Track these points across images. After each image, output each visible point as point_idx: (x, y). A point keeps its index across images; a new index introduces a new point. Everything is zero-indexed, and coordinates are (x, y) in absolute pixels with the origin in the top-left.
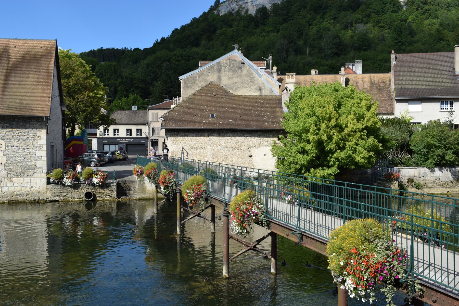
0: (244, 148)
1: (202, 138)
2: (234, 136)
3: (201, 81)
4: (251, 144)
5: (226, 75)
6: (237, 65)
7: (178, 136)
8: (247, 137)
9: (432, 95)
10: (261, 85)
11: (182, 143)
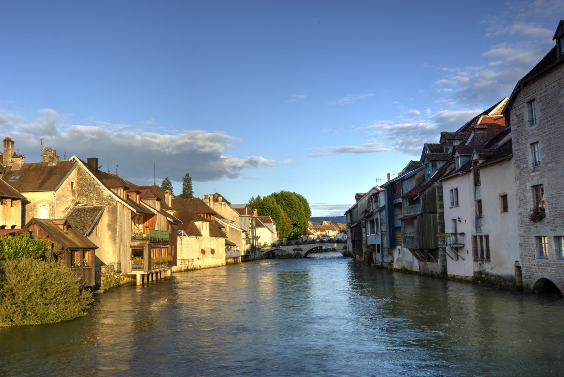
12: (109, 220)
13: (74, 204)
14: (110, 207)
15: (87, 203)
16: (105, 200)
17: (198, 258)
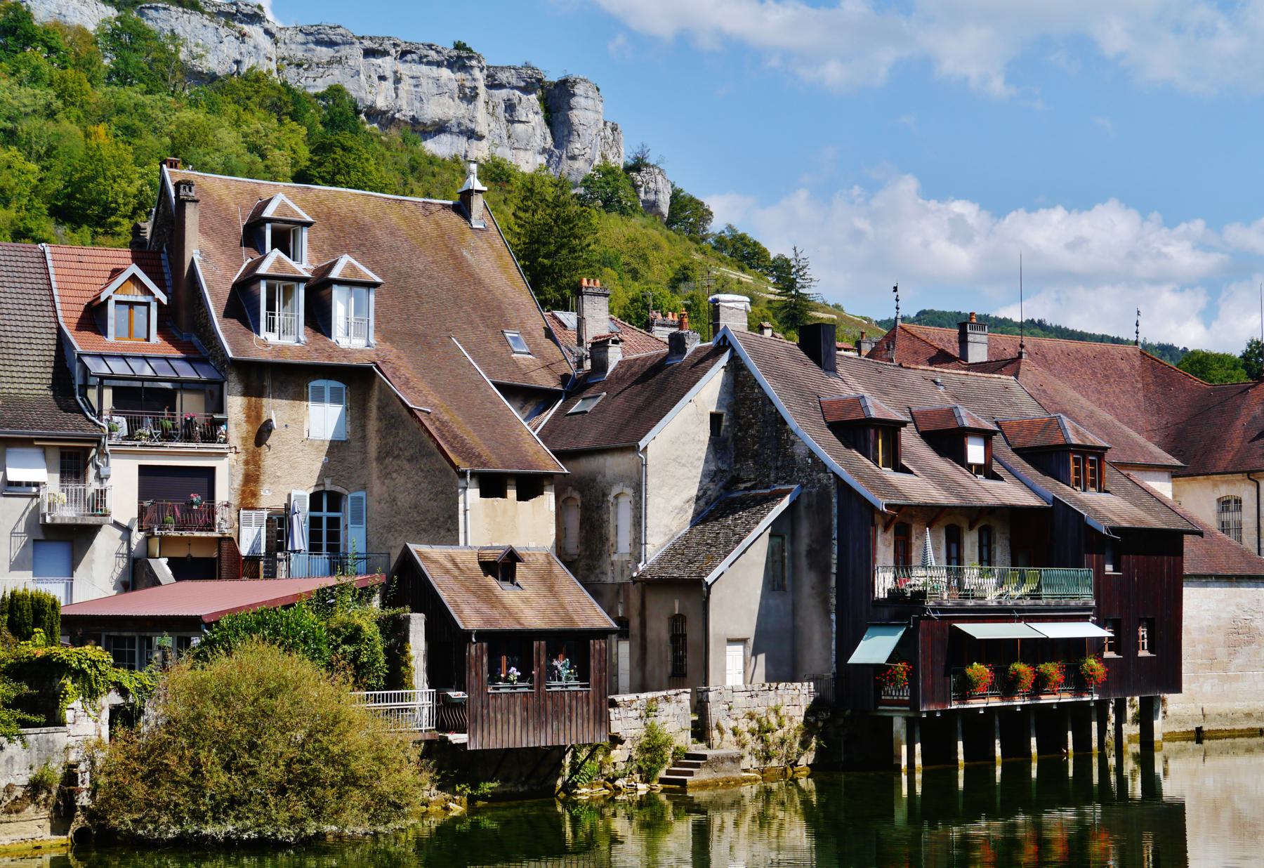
12: (811, 535)
13: (721, 484)
14: (814, 490)
15: (755, 479)
16: (799, 470)
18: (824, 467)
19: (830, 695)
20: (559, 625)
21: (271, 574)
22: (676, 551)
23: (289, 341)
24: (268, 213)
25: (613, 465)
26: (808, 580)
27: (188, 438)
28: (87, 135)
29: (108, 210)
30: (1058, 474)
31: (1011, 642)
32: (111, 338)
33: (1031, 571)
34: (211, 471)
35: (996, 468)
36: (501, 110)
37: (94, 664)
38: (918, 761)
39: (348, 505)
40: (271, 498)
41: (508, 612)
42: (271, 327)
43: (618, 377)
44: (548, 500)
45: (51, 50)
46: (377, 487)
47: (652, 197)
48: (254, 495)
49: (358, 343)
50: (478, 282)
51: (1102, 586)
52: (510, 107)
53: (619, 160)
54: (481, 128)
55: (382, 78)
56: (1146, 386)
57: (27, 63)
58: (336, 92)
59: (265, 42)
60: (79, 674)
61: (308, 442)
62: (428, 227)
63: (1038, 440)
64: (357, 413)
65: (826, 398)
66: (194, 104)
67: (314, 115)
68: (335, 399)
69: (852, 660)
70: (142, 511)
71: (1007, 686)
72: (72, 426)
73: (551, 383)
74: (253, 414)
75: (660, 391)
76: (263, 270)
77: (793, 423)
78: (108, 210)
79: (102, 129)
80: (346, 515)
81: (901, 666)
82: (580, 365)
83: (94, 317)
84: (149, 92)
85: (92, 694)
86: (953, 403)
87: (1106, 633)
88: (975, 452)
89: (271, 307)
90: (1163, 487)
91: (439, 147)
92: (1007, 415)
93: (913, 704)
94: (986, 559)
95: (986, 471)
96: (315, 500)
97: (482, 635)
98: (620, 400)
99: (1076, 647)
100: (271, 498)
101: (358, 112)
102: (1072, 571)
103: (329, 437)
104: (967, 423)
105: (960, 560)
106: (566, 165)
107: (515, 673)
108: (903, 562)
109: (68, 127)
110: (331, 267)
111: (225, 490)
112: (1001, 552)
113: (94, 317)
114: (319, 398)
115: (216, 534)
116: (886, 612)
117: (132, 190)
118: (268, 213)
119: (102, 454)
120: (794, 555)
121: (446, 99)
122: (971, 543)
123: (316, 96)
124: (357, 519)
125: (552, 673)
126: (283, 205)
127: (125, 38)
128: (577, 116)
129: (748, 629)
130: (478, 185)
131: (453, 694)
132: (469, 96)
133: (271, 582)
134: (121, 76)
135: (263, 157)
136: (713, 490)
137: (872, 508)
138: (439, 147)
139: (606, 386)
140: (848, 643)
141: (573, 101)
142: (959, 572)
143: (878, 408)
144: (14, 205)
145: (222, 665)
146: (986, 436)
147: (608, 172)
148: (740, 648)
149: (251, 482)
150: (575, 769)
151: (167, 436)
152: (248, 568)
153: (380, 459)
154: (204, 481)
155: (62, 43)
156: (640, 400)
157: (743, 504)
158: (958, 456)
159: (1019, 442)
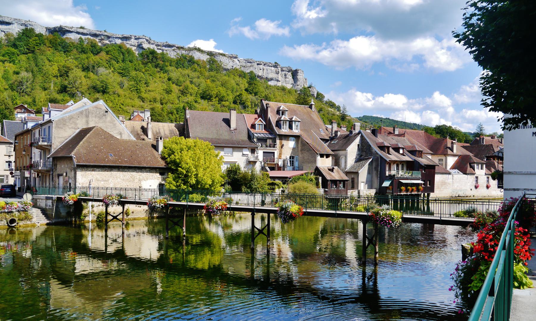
0: (136, 181)
1: (106, 173)
2: (129, 171)
3: (71, 124)
4: (141, 177)
5: (93, 120)
6: (102, 112)
7: (87, 170)
8: (138, 172)
9: (219, 143)
10: (121, 131)
11: (91, 176)
17: (471, 190)
18: (378, 154)
19: (378, 192)
20: (341, 179)
21: (284, 170)
22: (352, 167)
23: (286, 131)
24: (281, 109)
25: (341, 153)
26: (374, 172)
27: (270, 147)
28: (206, 82)
29: (211, 97)
30: (415, 155)
31: (408, 183)
32: (256, 130)
33: (411, 172)
34: (274, 153)
35: (404, 154)
36: (283, 76)
37: (280, 184)
38: (393, 203)
39: (295, 158)
40: (283, 157)
41: (334, 177)
42: (283, 129)
43: (340, 138)
44: (330, 158)
45: (198, 65)
46: (300, 156)
47: (313, 93)
48: (281, 156)
49: (297, 131)
50: (314, 120)
51: (422, 174)
52: (285, 75)
53: (306, 86)
54: (280, 79)
55: (260, 69)
56: (425, 138)
57: (194, 68)
58: (251, 72)
59: (238, 62)
60: (278, 185)
61: (290, 148)
62: (305, 111)
63: (411, 149)
64: (297, 143)
65: (377, 142)
66: (225, 75)
67: (248, 77)
68: (293, 141)
69: (383, 185)
70: (263, 159)
71: (407, 190)
72: (253, 145)
73: (328, 138)
74: (281, 143)
75: (349, 140)
76: (282, 119)
77: (372, 146)
78: (211, 97)
79: (209, 80)
80: (295, 160)
81: (391, 187)
82: (332, 135)
83: (253, 126)
84: (217, 73)
85: (279, 188)
86: (396, 143)
87: (423, 182)
88: (401, 151)
89: (283, 125)
90: (430, 157)
91: (271, 83)
92: (405, 145)
93: (392, 193)
94: (402, 169)
95: (403, 154)
96: (290, 157)
97: (330, 180)
98: (341, 142)
99: (417, 185)
100: (283, 157)
101: (256, 76)
102: (418, 172)
103: (292, 147)
104: (400, 146)
105: (398, 170)
106: (296, 87)
107: (335, 186)
108: (390, 169)
109: (202, 80)
110: (292, 118)
111: (276, 156)
112: (405, 168)
113: (253, 126)
114: (291, 141)
115: (275, 163)
116: (388, 178)
117: (215, 93)
118: (281, 109)
119: (257, 149)
120: (372, 168)
121: (273, 74)
122: (400, 166)
123: (248, 73)
124: (297, 161)
125: (340, 187)
126: (283, 107)
127: (211, 62)
128: (299, 77)
129: (365, 180)
130: (313, 103)
131: (326, 190)
132: (277, 73)
133: (284, 171)
134: (211, 70)
135: (239, 86)
136: (358, 157)
137: (386, 161)
138: (271, 83)
139: (337, 139)
140: (381, 183)
141: (298, 74)
142: (398, 172)
143: (386, 144)
144: (193, 96)
145: (296, 184)
146: (403, 149)
147: (305, 88)
148: (363, 183)
149: (280, 154)
150: (341, 202)
151: (267, 147)
152: (279, 169)
153: (301, 151)
154: (273, 154)
155: (200, 63)
156: (345, 142)
157: (363, 160)
158: (398, 152)
159: (408, 150)
